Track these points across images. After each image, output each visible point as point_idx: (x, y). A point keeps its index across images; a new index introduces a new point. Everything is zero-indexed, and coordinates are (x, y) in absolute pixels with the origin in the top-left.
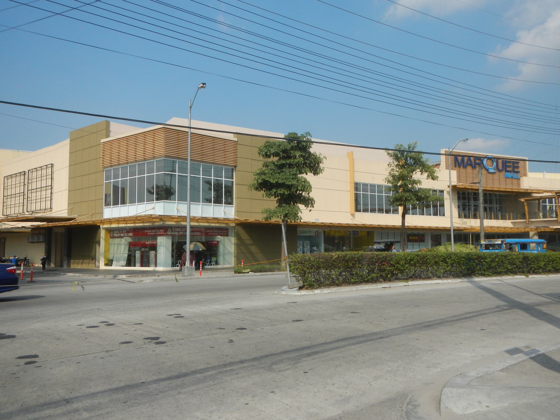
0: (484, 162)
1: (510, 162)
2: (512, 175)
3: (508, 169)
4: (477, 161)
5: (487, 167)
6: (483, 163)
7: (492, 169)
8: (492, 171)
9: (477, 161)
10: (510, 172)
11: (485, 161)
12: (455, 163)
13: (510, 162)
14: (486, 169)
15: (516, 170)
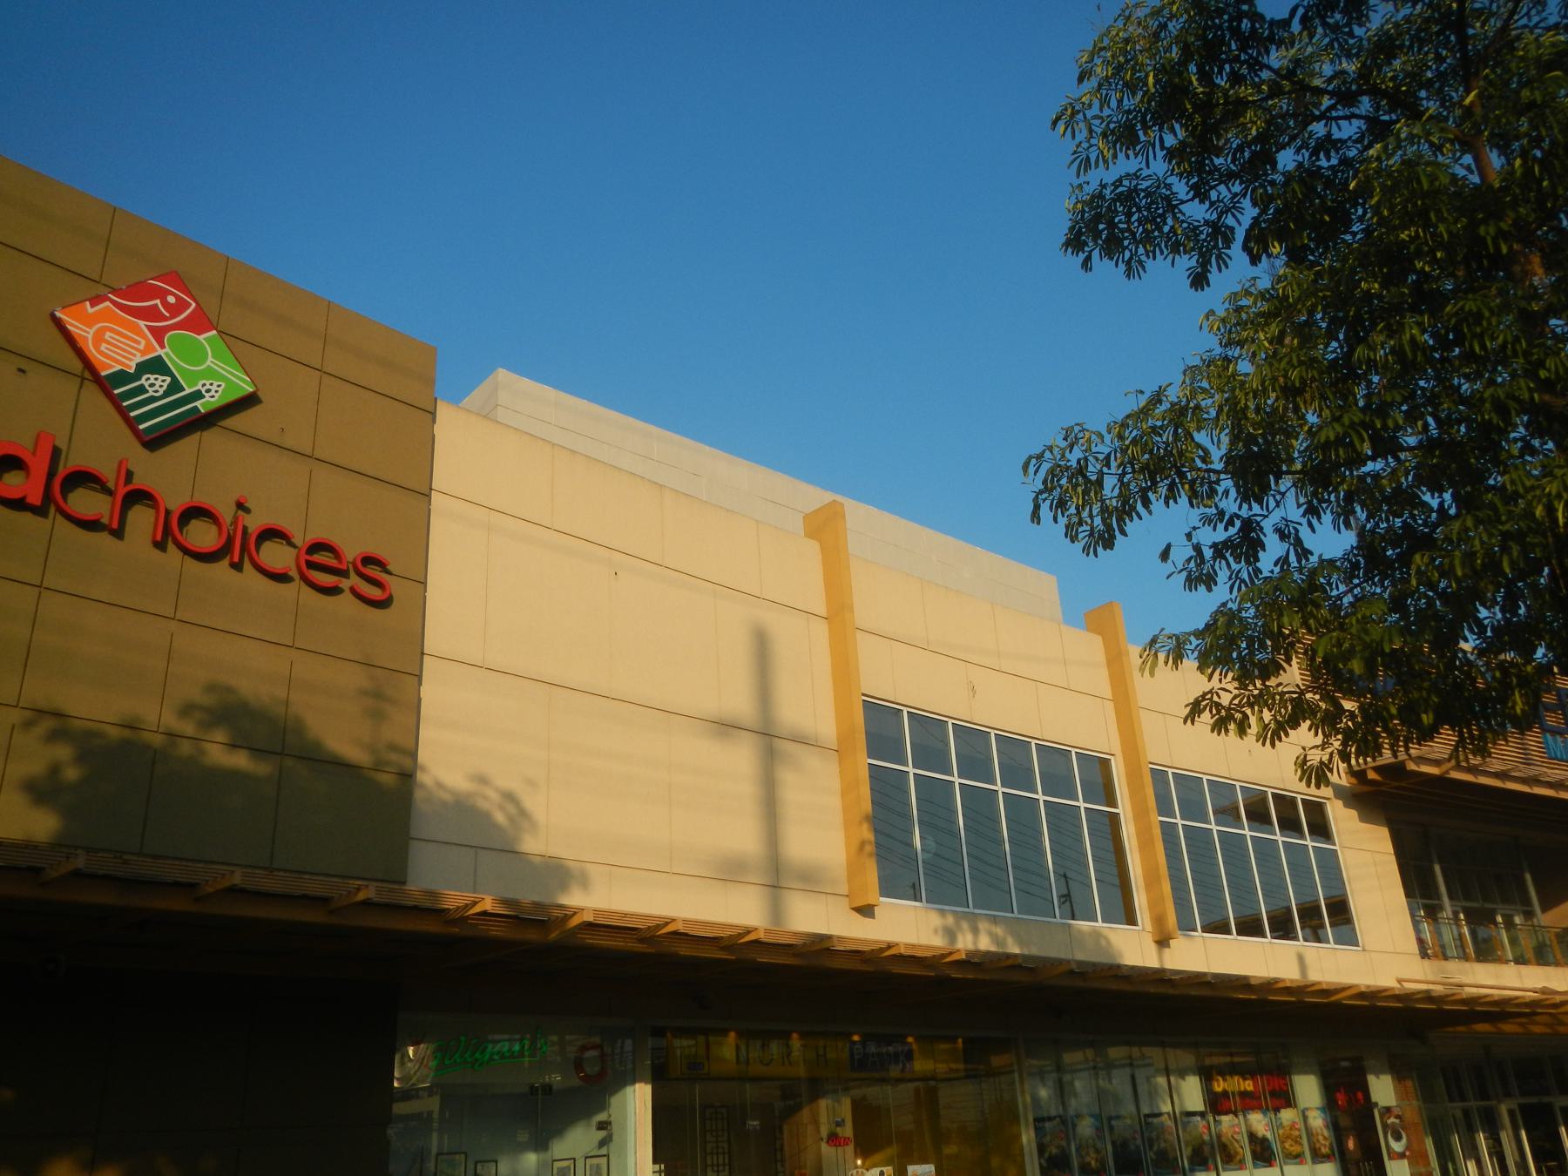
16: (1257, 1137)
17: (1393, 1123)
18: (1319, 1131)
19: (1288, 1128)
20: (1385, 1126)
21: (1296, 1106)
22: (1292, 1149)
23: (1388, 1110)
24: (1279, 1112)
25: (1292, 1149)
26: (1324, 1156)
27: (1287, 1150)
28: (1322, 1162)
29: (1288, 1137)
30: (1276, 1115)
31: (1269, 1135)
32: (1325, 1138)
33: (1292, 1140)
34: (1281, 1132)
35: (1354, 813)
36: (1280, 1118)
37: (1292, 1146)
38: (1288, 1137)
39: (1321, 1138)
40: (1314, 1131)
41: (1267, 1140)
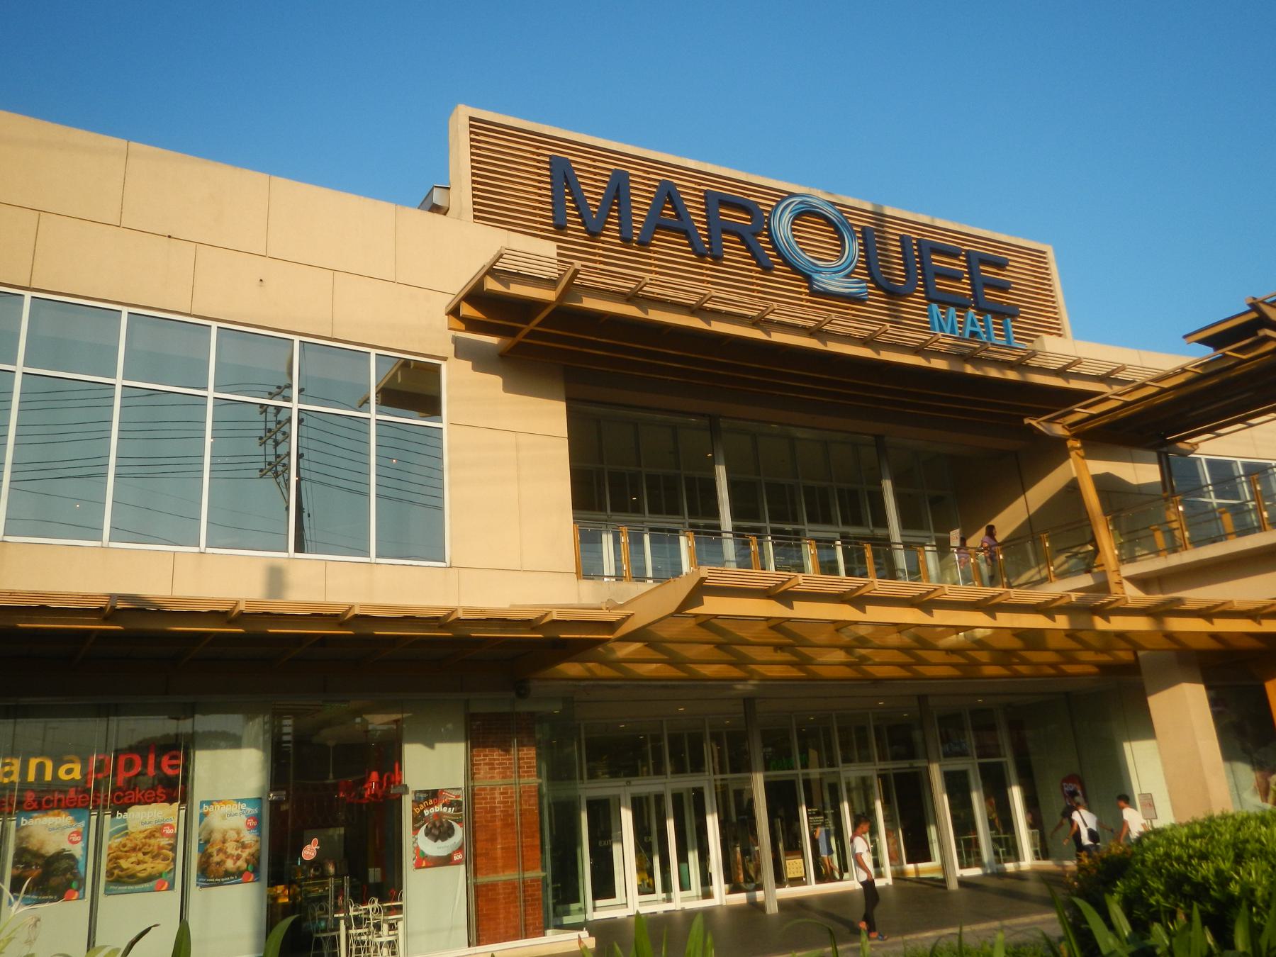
0: (775, 224)
1: (953, 253)
2: (973, 324)
3: (942, 285)
4: (730, 216)
5: (804, 259)
6: (769, 229)
7: (838, 277)
8: (836, 284)
9: (730, 216)
10: (962, 306)
11: (783, 227)
12: (557, 204)
13: (953, 253)
14: (795, 270)
15: (991, 295)
16: (37, 855)
17: (438, 815)
18: (232, 835)
19: (142, 835)
20: (418, 819)
21: (185, 799)
22: (139, 868)
23: (434, 795)
24: (124, 811)
25: (139, 868)
26: (227, 874)
27: (122, 870)
28: (221, 884)
29: (134, 849)
30: (114, 815)
31: (77, 850)
32: (244, 846)
33: (145, 854)
34: (116, 842)
35: (496, 381)
36: (125, 821)
37: (139, 863)
38: (134, 849)
39: (231, 848)
40: (217, 836)
41: (71, 857)
